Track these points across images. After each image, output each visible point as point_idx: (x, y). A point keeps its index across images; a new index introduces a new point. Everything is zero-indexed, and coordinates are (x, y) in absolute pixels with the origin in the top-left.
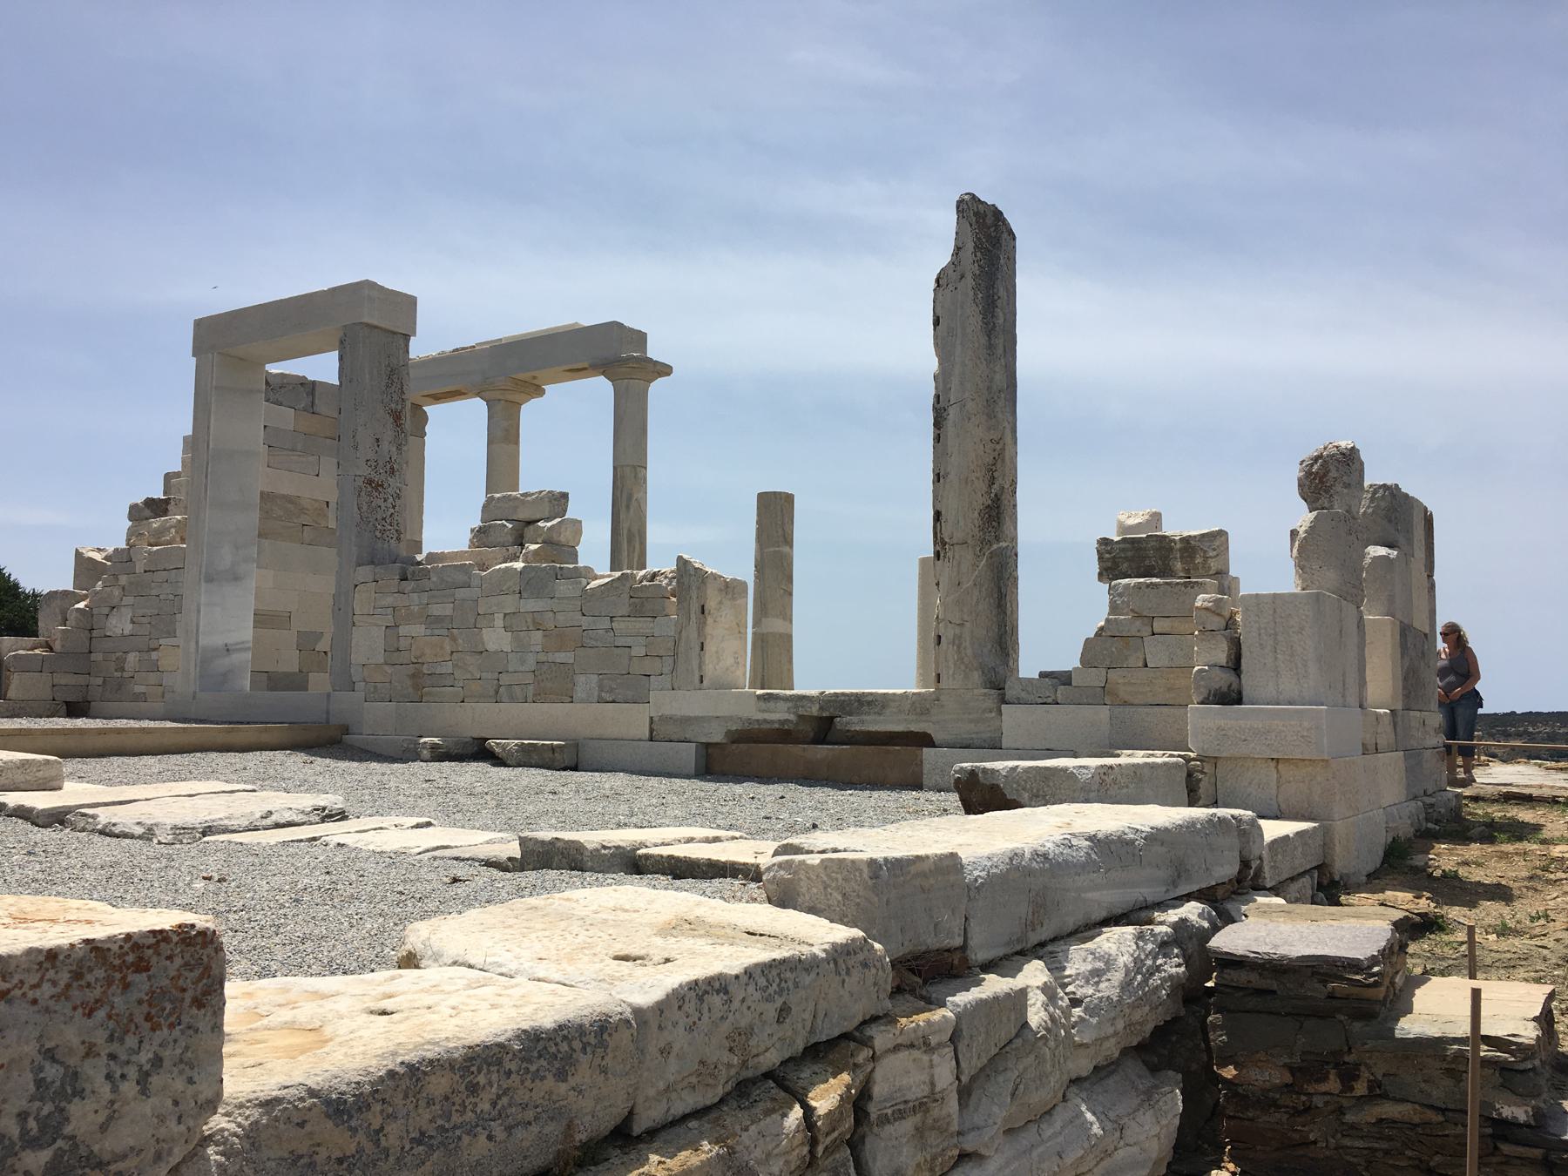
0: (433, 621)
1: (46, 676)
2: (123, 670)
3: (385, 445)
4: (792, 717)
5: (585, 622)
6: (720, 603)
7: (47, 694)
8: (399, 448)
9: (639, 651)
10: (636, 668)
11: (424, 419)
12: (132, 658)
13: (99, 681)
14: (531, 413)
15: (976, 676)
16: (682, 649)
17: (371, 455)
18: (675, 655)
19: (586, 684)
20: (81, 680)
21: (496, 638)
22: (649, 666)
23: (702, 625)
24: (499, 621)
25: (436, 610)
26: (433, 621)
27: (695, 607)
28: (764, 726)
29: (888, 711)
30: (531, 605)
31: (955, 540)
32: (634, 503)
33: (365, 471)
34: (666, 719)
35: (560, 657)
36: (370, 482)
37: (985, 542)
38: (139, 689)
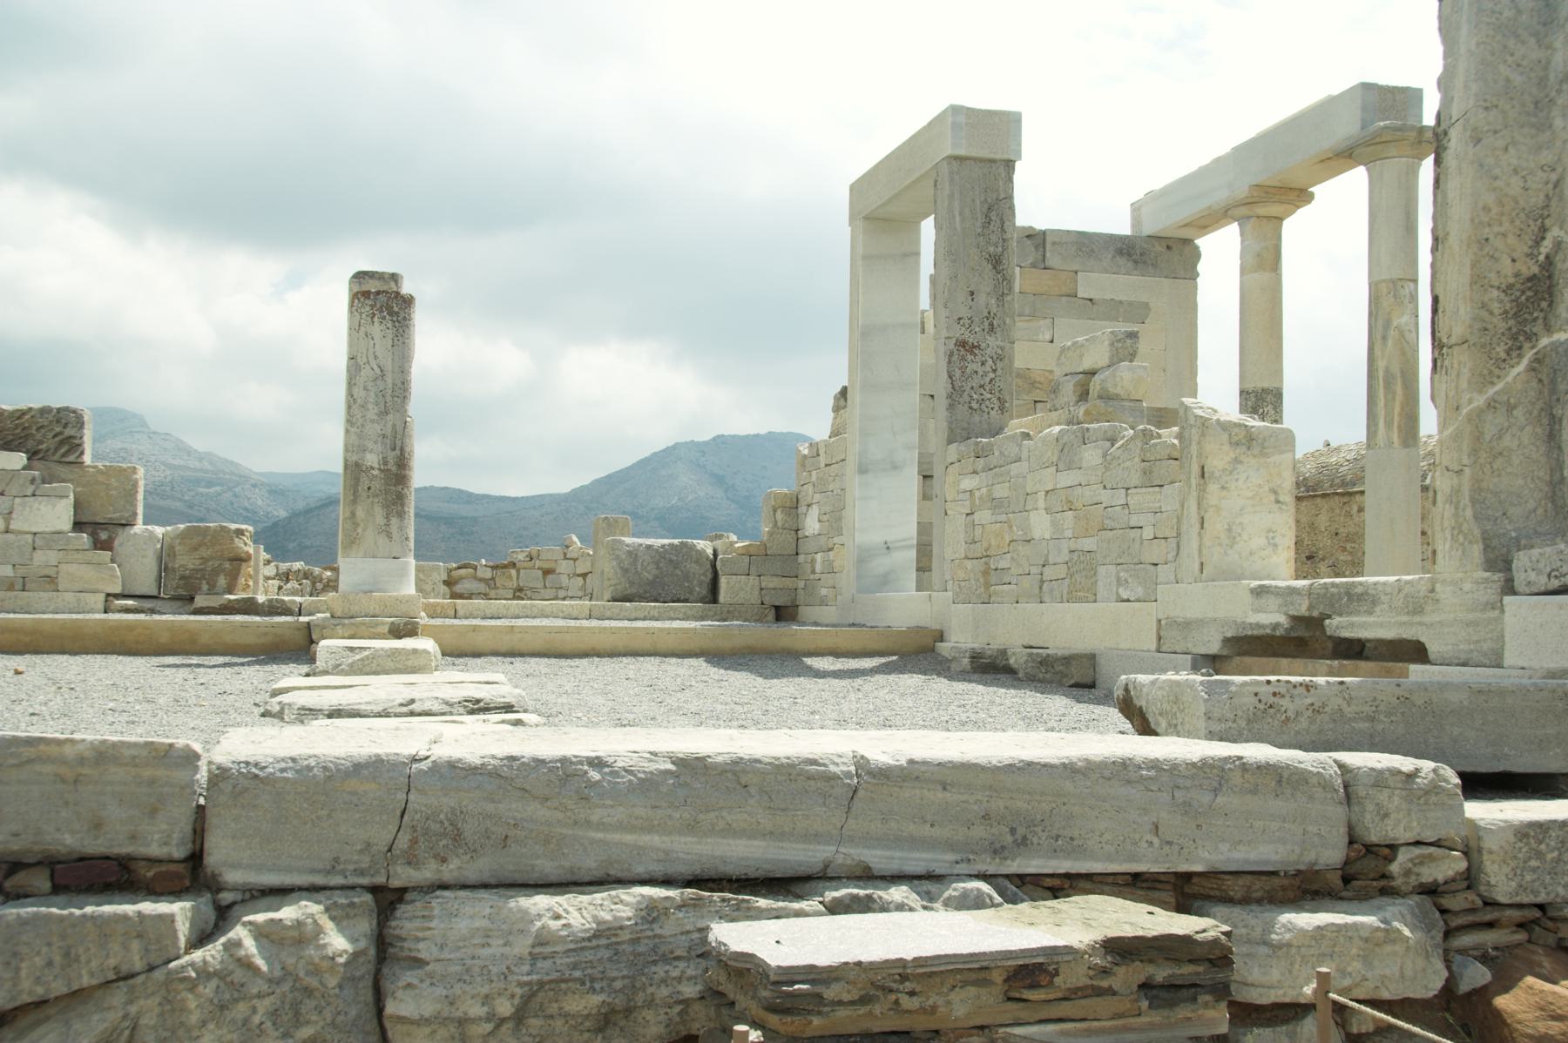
0: (996, 504)
1: (753, 580)
2: (813, 572)
3: (982, 299)
4: (1282, 619)
5: (1105, 496)
6: (1236, 461)
7: (754, 598)
8: (1001, 297)
9: (1148, 533)
10: (1149, 557)
11: (1196, 255)
12: (819, 557)
13: (801, 584)
14: (1297, 228)
15: (1477, 550)
16: (1184, 528)
17: (964, 312)
18: (1179, 535)
19: (1106, 574)
20: (788, 582)
21: (1040, 524)
22: (1156, 552)
23: (1202, 490)
24: (1041, 504)
25: (1001, 491)
26: (996, 504)
27: (1195, 469)
28: (1255, 632)
29: (1377, 609)
30: (1066, 479)
31: (1453, 340)
32: (1392, 333)
33: (959, 332)
34: (1173, 623)
35: (1088, 544)
36: (962, 344)
37: (1519, 338)
38: (824, 592)
